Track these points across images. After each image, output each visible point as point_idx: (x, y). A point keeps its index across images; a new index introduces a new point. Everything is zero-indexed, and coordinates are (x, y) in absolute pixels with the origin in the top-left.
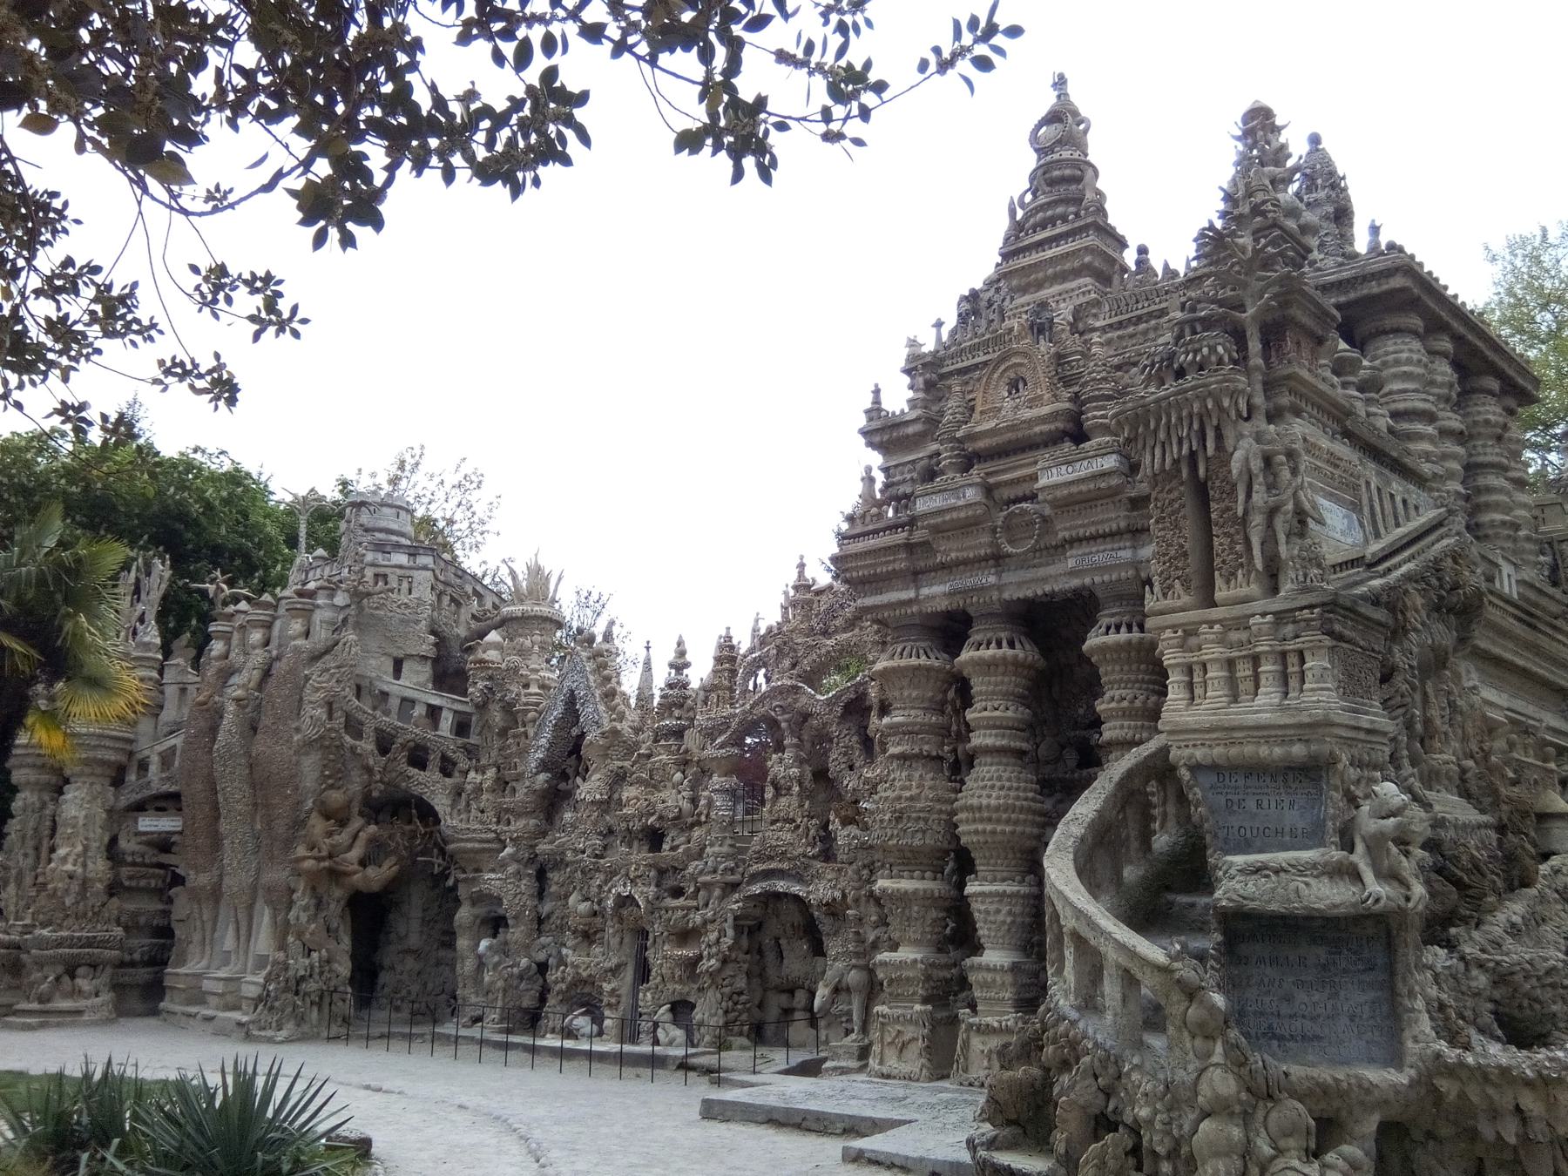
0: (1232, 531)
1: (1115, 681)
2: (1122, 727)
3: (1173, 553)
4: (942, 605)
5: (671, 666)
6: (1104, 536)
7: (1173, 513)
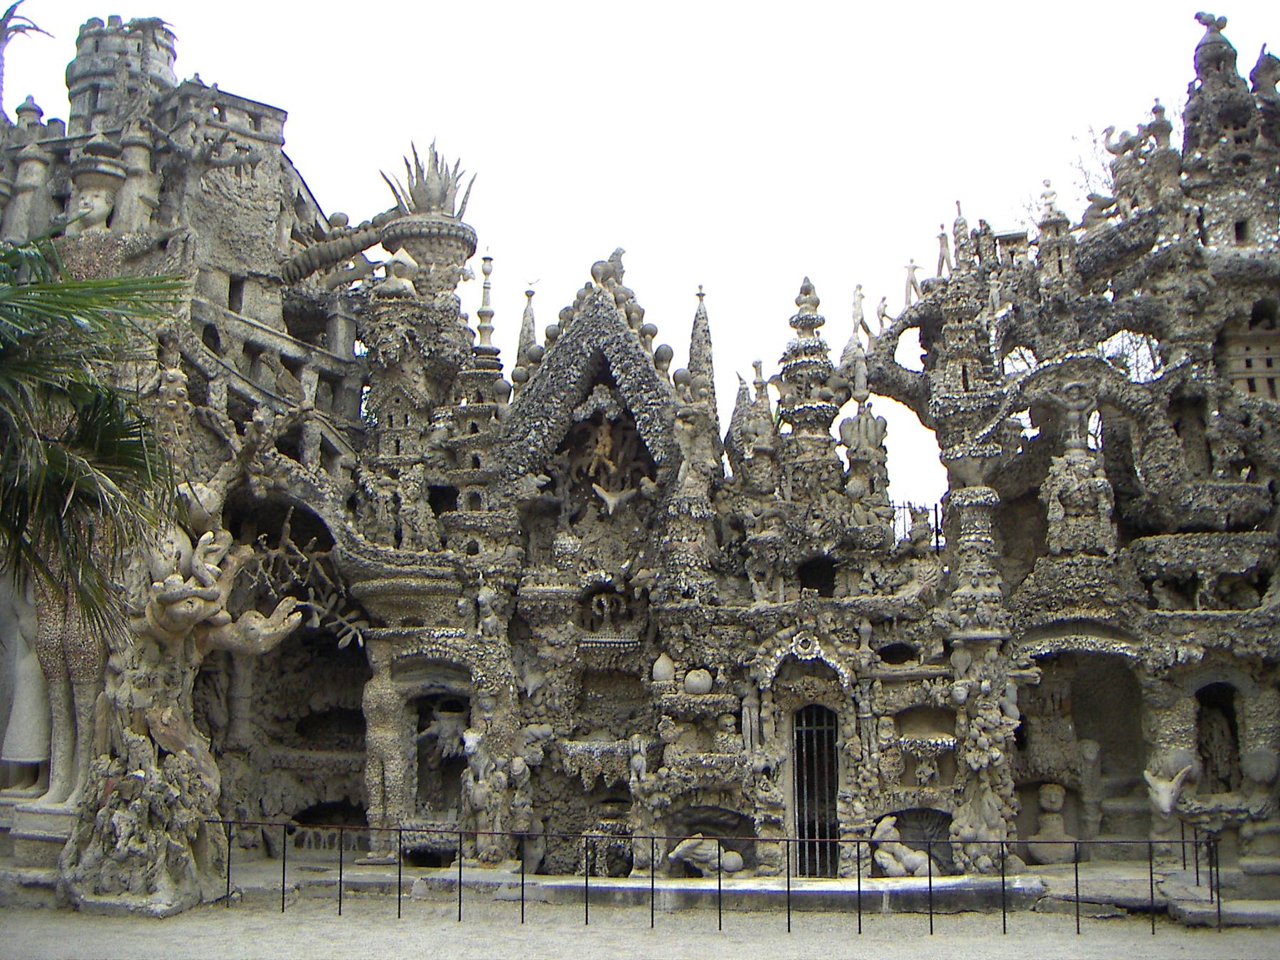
5: (794, 323)
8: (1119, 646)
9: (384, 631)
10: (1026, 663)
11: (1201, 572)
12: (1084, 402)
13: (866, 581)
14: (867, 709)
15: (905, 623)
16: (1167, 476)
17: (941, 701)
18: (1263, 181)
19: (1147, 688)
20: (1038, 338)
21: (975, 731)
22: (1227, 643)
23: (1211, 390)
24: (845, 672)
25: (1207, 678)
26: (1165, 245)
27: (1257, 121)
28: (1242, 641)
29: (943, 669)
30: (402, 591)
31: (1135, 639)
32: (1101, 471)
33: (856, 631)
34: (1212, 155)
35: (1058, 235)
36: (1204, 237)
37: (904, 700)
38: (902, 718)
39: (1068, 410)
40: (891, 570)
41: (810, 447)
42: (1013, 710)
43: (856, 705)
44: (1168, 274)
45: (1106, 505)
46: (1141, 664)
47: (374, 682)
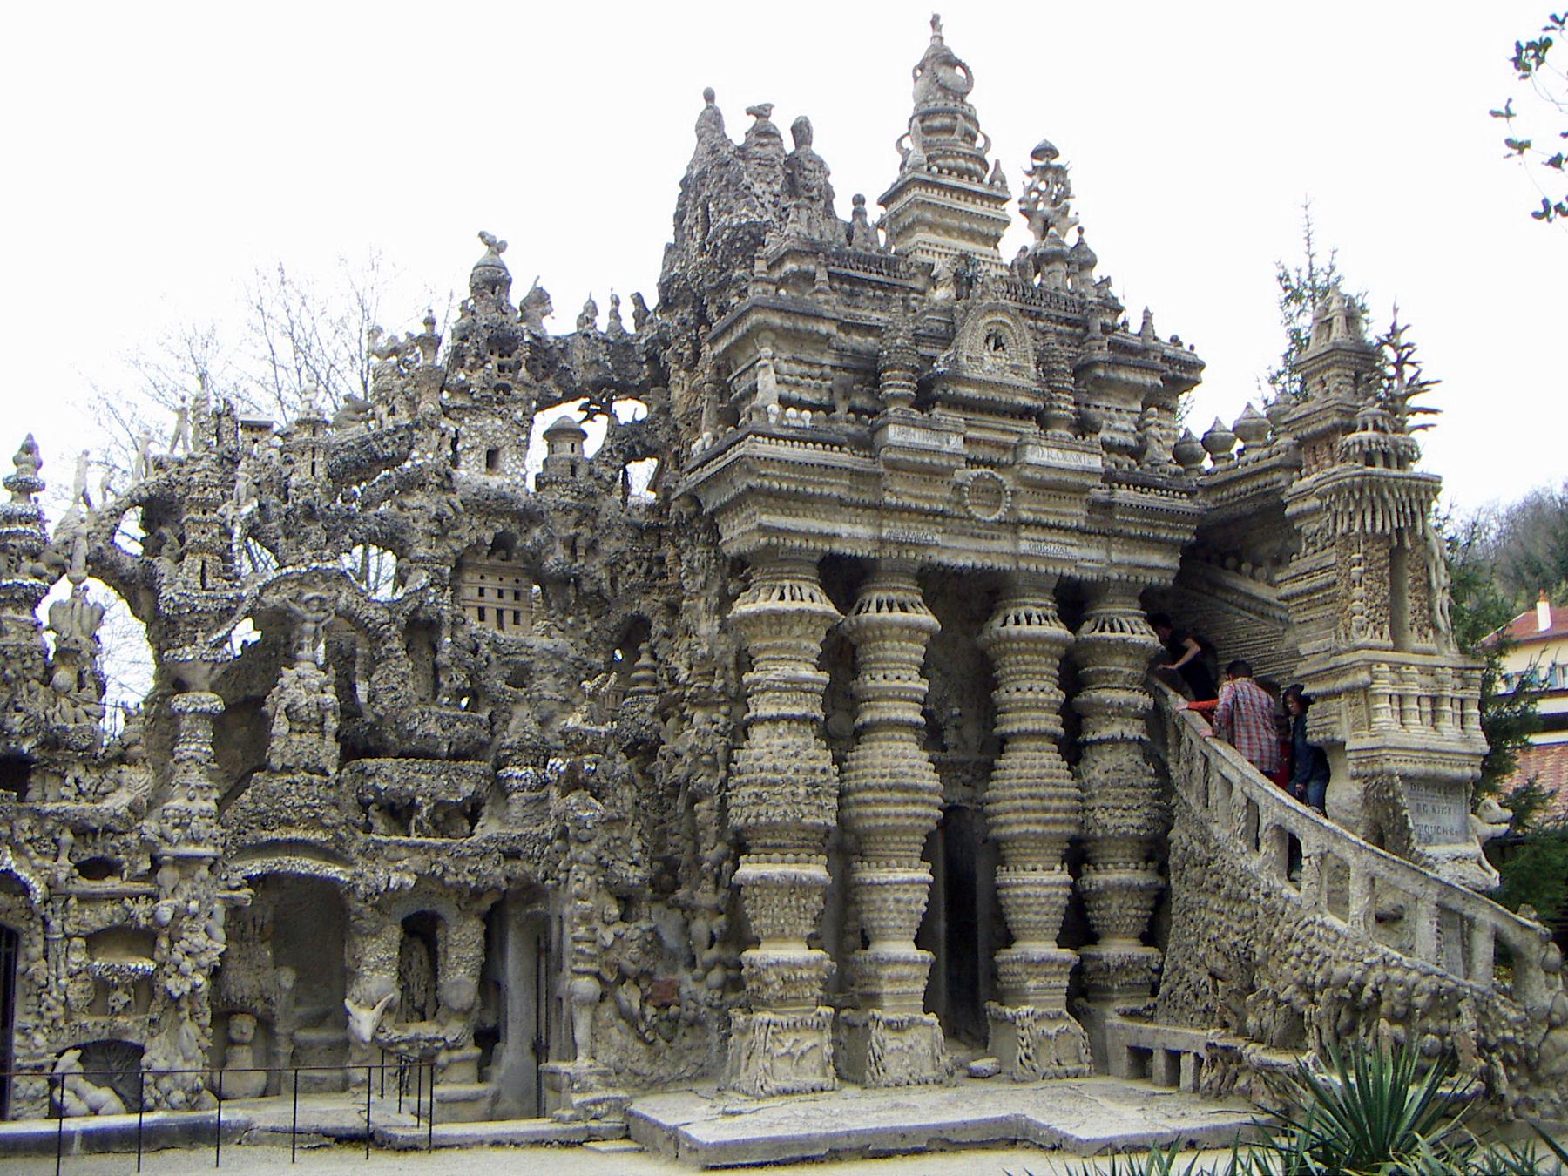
0: (1422, 596)
1: (1042, 674)
2: (1047, 719)
3: (1378, 601)
4: (864, 551)
5: (8, 485)
6: (1059, 528)
7: (1380, 569)
8: (333, 871)
10: (237, 884)
11: (420, 798)
12: (322, 615)
13: (69, 786)
14: (58, 929)
15: (110, 835)
16: (396, 699)
17: (143, 922)
18: (520, 414)
19: (355, 914)
20: (282, 541)
21: (178, 956)
22: (439, 871)
23: (447, 616)
24: (39, 889)
26: (419, 462)
27: (524, 353)
28: (453, 870)
29: (148, 887)
31: (349, 863)
32: (331, 688)
33: (55, 841)
34: (476, 379)
35: (314, 435)
36: (455, 462)
37: (101, 920)
38: (95, 941)
39: (305, 621)
40: (96, 776)
41: (14, 629)
42: (220, 933)
43: (46, 924)
44: (417, 492)
45: (332, 723)
46: (353, 889)
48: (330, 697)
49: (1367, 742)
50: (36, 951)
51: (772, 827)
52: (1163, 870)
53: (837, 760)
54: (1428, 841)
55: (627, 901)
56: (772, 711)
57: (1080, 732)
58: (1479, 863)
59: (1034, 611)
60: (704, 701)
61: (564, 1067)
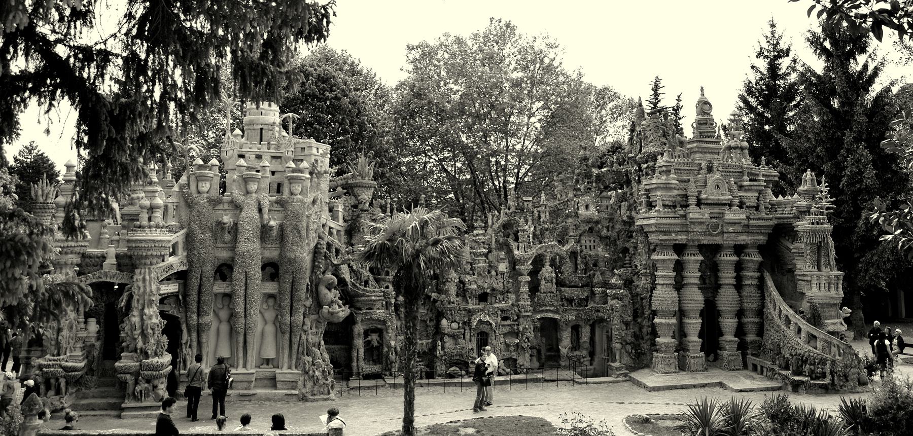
8: (556, 316)
9: (362, 312)
25: (574, 323)
30: (371, 301)
34: (582, 187)
36: (578, 209)
45: (554, 281)
46: (560, 320)
47: (357, 326)
48: (554, 275)
49: (810, 294)
50: (493, 338)
51: (663, 311)
52: (762, 318)
53: (678, 294)
54: (826, 319)
55: (627, 324)
56: (662, 282)
57: (741, 281)
58: (842, 324)
59: (728, 253)
60: (645, 275)
61: (613, 364)
